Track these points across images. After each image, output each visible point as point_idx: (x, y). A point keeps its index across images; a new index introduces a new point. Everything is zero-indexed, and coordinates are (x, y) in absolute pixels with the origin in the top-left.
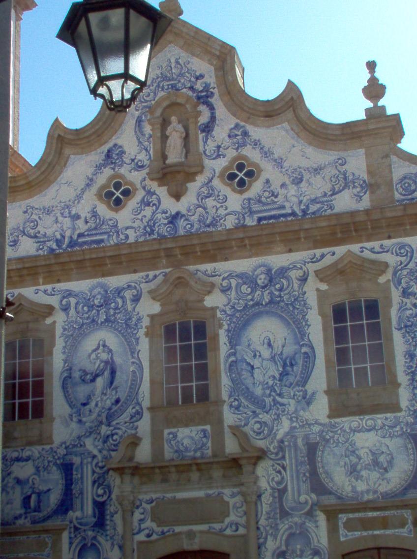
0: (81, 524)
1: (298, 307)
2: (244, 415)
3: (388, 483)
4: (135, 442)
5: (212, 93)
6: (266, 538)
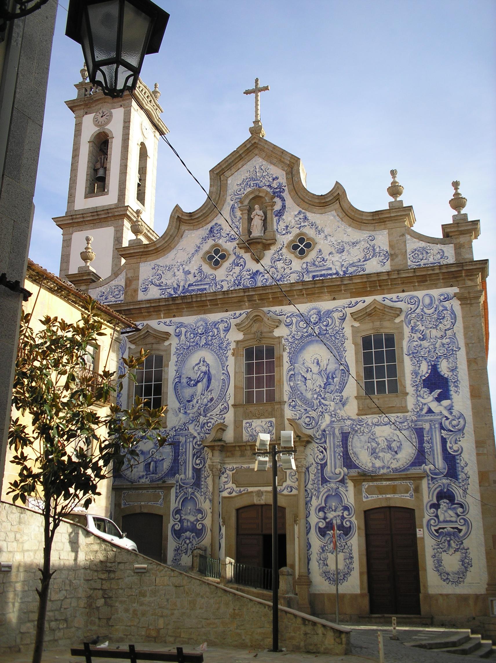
0: (184, 483)
4: (222, 428)
5: (283, 189)
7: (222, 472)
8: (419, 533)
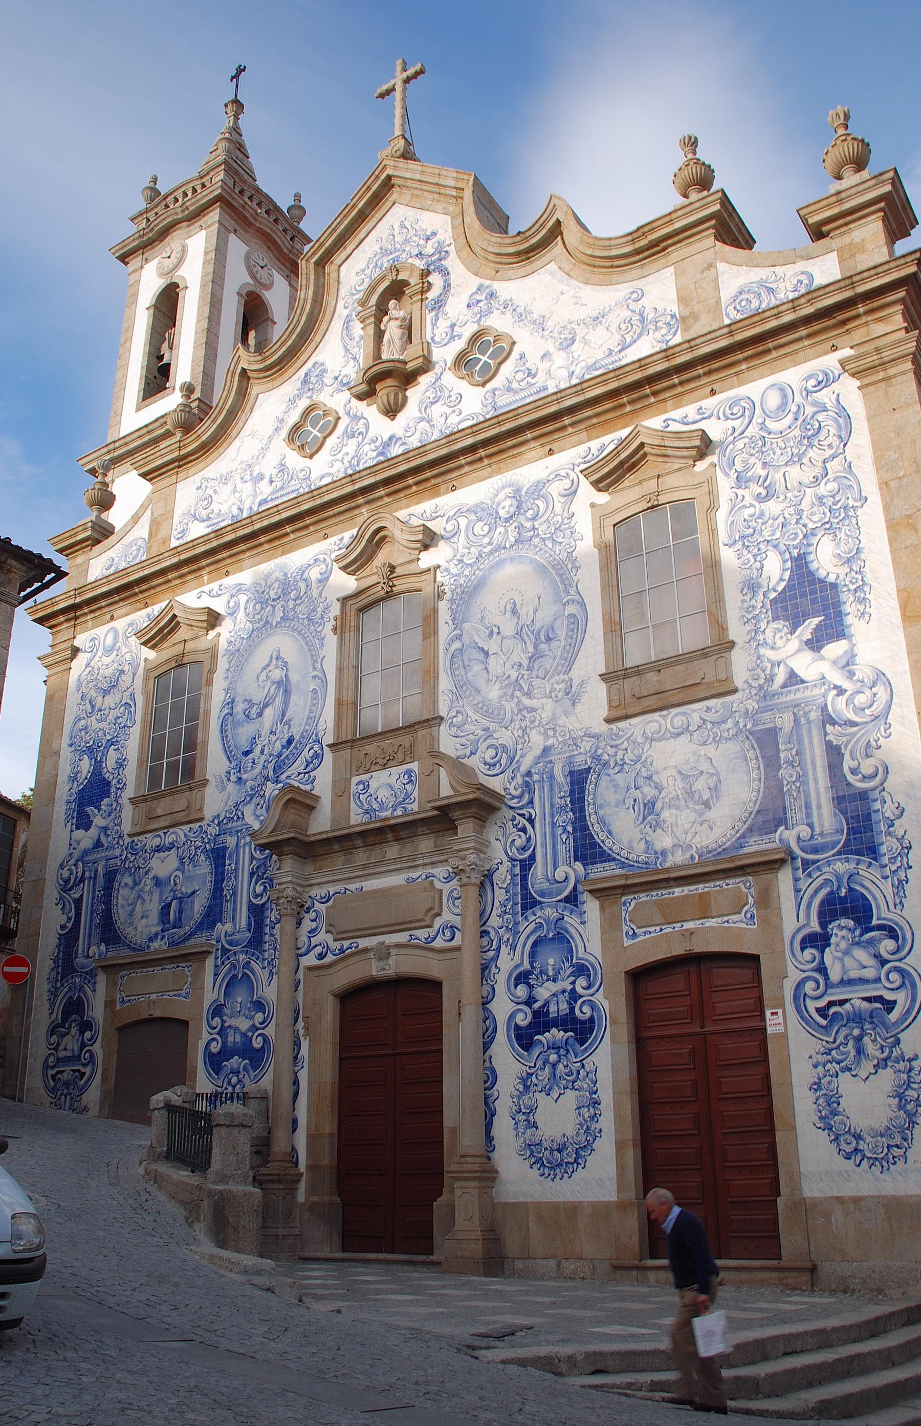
0: (230, 943)
1: (561, 540)
2: (471, 737)
3: (711, 829)
5: (447, 252)
6: (499, 949)
7: (301, 908)
8: (773, 1024)
